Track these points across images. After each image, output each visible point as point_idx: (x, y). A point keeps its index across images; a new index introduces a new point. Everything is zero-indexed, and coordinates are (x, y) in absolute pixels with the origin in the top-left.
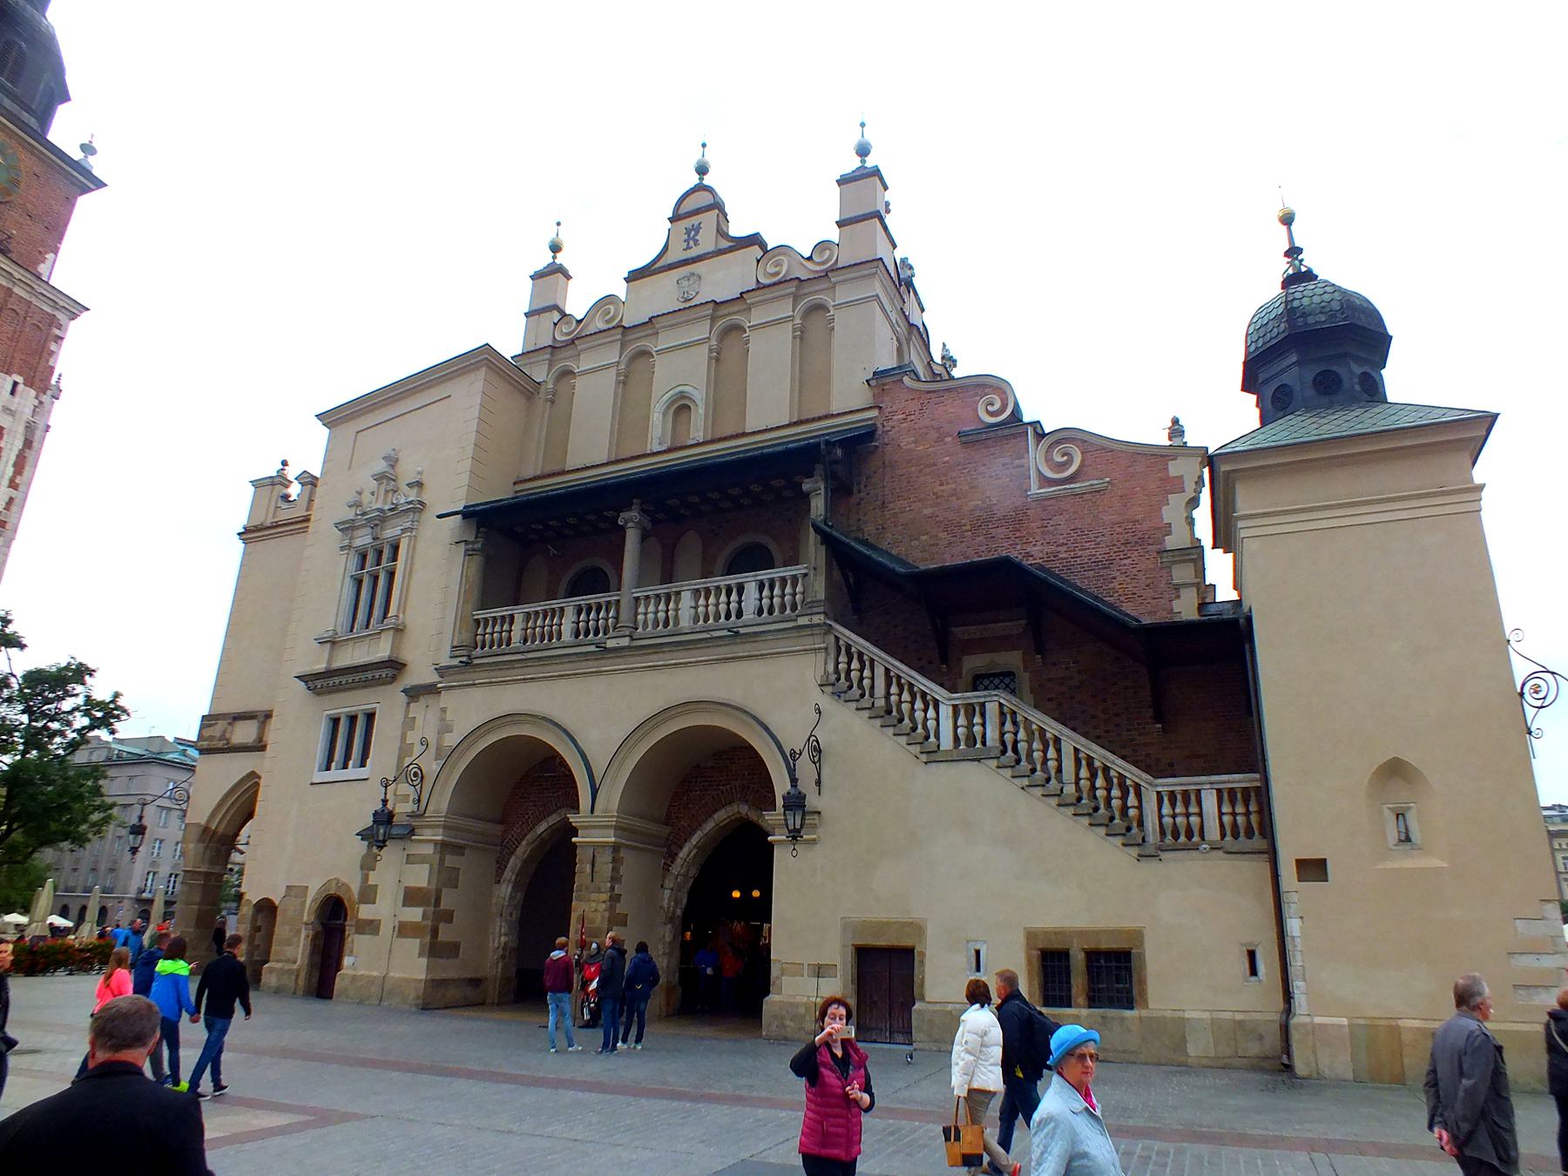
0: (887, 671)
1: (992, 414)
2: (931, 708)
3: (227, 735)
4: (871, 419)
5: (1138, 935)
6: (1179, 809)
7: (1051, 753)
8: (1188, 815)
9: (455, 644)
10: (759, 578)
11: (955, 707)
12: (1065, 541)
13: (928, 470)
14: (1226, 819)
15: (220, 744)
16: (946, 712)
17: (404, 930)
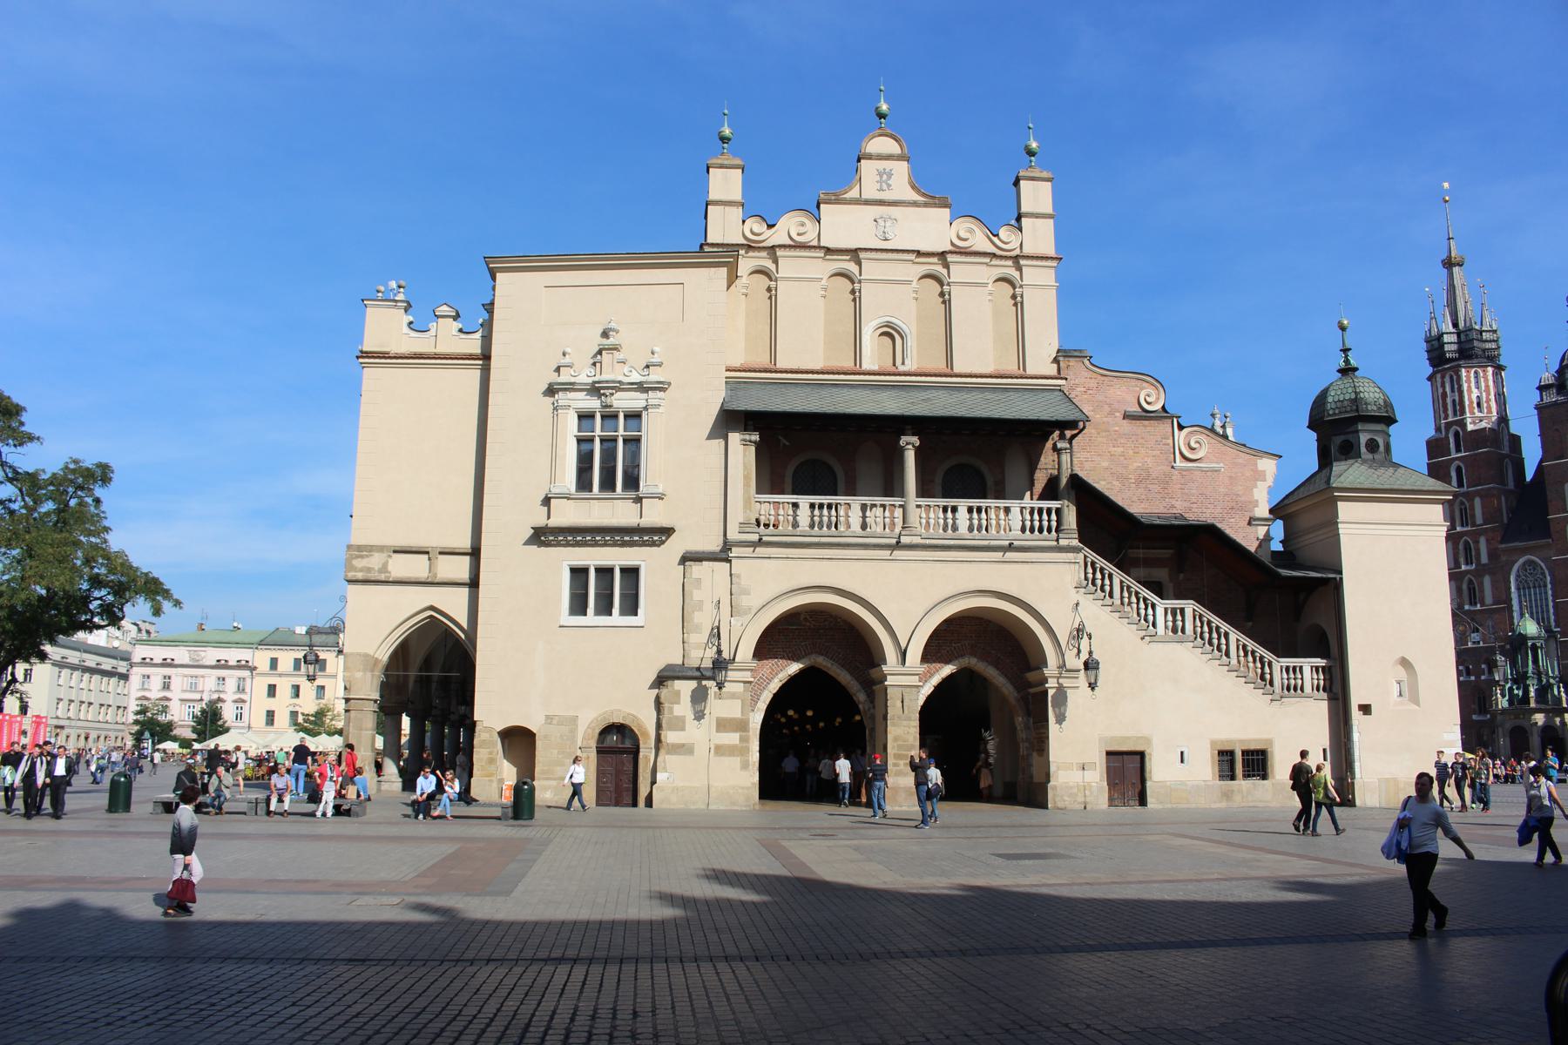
0: (1122, 582)
1: (1148, 403)
2: (1150, 607)
3: (390, 568)
4: (1060, 386)
5: (1270, 742)
6: (1292, 676)
7: (1223, 641)
8: (1295, 679)
9: (742, 521)
10: (1023, 505)
11: (1166, 610)
12: (1195, 501)
13: (1104, 434)
14: (1316, 682)
15: (382, 577)
16: (1160, 611)
17: (720, 750)
